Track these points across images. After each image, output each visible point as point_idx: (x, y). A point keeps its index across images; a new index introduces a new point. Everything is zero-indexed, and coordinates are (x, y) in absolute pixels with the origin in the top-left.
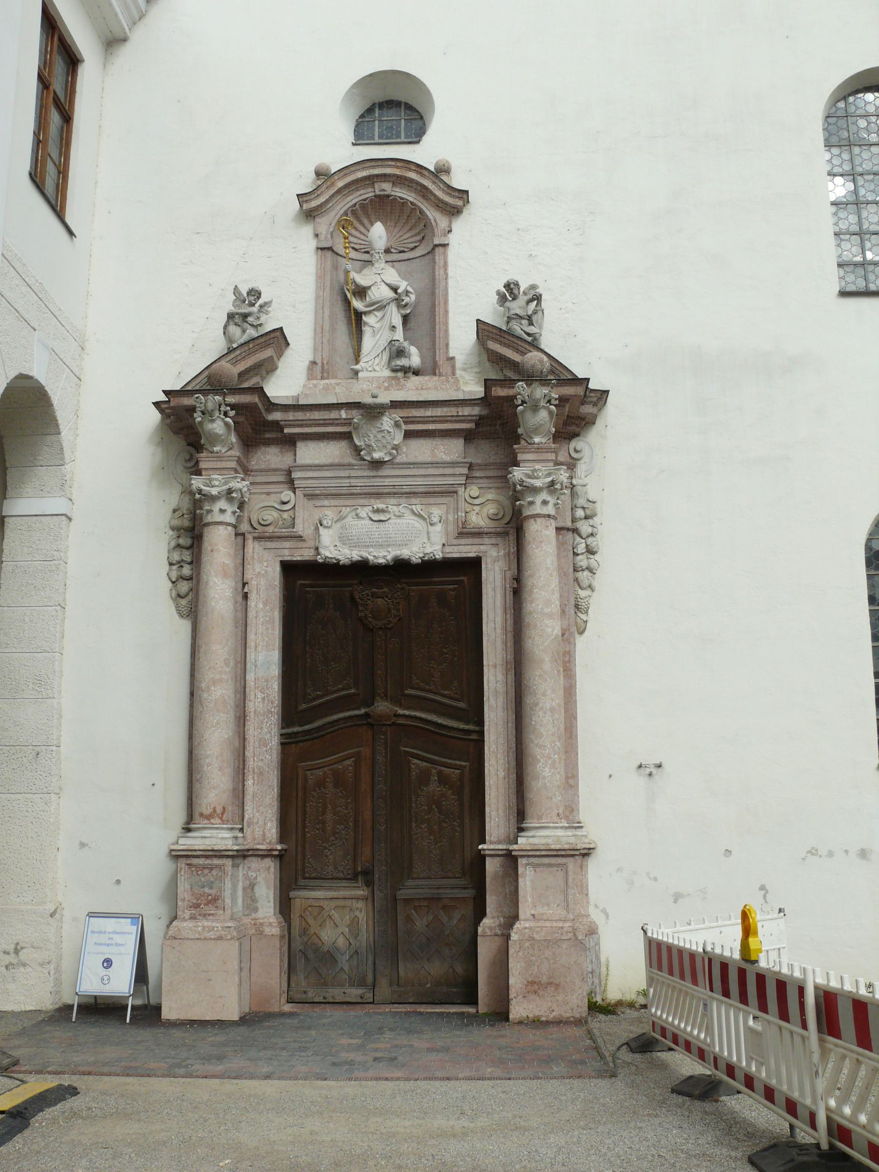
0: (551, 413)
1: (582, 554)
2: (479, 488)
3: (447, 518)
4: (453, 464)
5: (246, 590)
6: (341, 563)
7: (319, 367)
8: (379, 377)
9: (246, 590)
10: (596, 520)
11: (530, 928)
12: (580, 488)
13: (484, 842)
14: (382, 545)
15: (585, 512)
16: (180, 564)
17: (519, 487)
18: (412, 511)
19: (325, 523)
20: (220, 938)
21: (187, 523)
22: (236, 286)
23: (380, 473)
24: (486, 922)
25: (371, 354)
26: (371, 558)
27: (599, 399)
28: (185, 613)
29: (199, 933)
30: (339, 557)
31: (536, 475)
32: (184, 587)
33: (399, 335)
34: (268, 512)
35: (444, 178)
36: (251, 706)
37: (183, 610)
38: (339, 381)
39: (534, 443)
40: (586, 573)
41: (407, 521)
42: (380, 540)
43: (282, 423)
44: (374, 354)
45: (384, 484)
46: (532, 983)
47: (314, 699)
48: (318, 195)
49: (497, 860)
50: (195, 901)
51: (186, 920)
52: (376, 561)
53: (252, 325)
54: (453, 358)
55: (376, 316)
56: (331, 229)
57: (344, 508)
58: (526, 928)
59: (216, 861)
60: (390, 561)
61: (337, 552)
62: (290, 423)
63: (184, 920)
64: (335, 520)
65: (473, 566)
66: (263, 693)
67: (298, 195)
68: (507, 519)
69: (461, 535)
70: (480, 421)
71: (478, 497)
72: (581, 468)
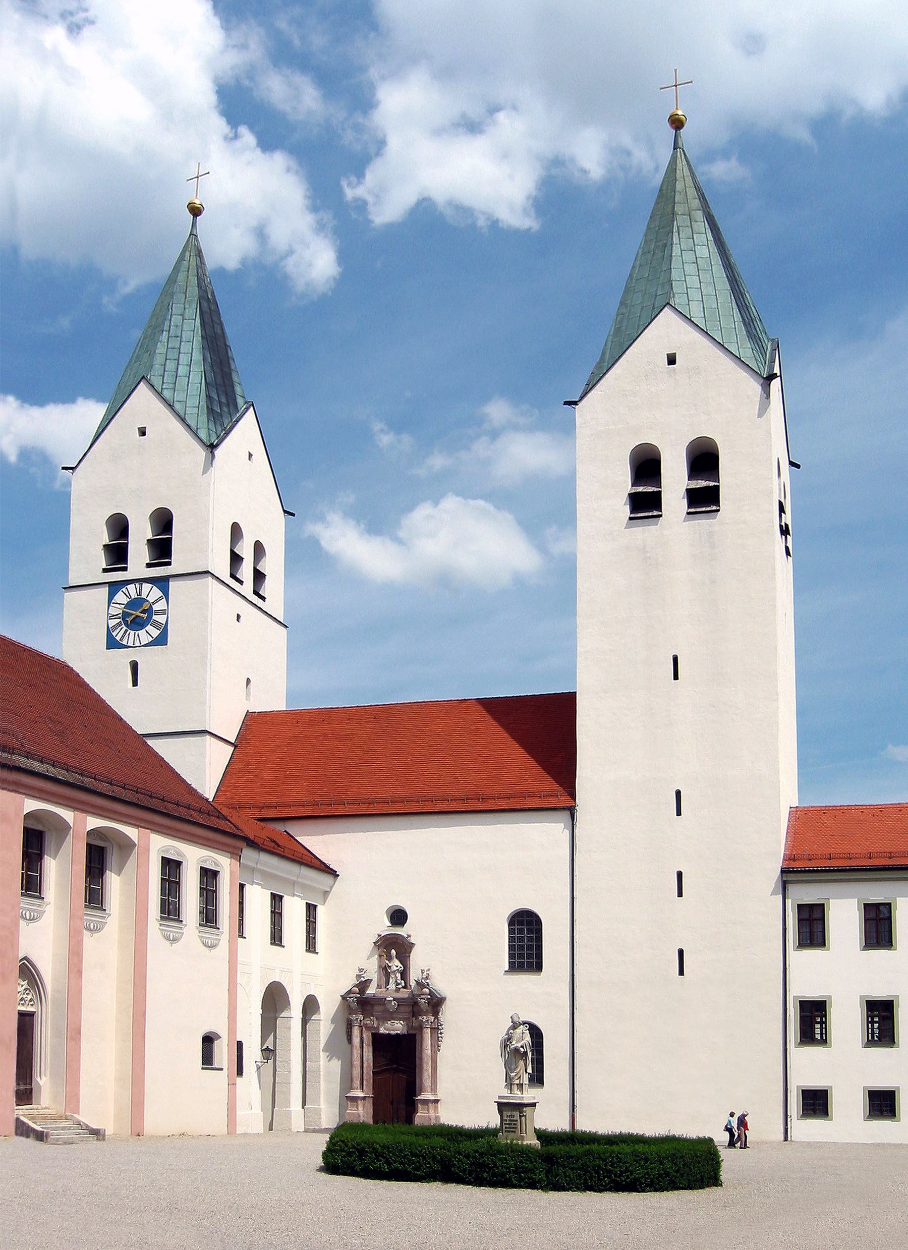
65: (415, 1035)
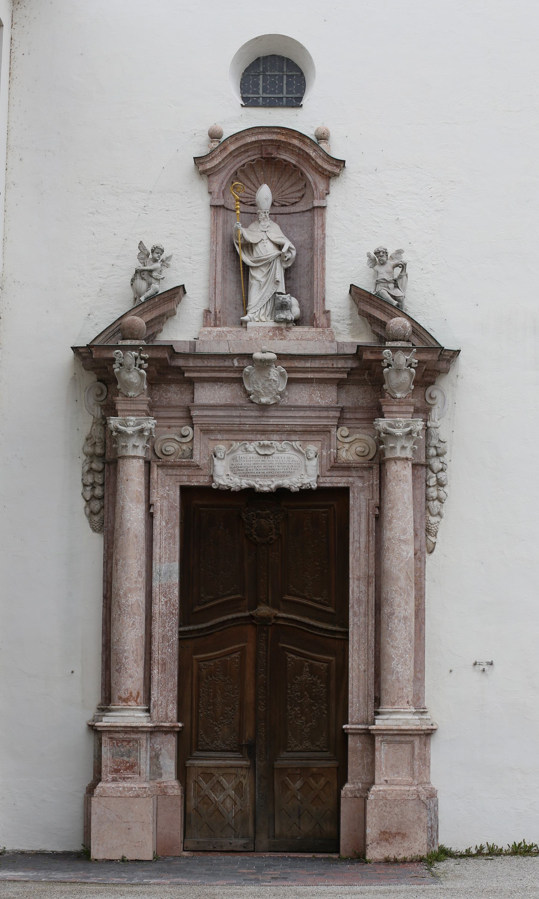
0: (411, 374)
1: (434, 486)
2: (348, 428)
3: (322, 453)
4: (327, 408)
5: (151, 511)
6: (232, 489)
7: (213, 316)
8: (265, 327)
9: (151, 511)
10: (446, 458)
11: (384, 791)
12: (433, 429)
13: (347, 723)
14: (267, 476)
15: (436, 450)
16: (93, 486)
17: (383, 435)
18: (293, 446)
19: (219, 455)
20: (138, 796)
21: (99, 450)
22: (141, 242)
23: (266, 414)
24: (348, 786)
25: (258, 306)
26: (257, 486)
27: (452, 357)
28: (97, 527)
29: (120, 792)
30: (231, 485)
31: (397, 425)
32: (96, 505)
33: (282, 288)
34: (171, 444)
35: (323, 145)
36: (156, 609)
37: (96, 525)
38: (230, 329)
39: (396, 398)
40: (436, 503)
41: (288, 455)
42: (266, 471)
43: (182, 368)
44: (260, 305)
45: (269, 423)
46: (384, 833)
47: (206, 603)
48: (213, 158)
49: (357, 738)
50: (116, 767)
51: (109, 782)
52: (261, 489)
53: (156, 279)
54: (328, 312)
55: (263, 271)
56: (223, 188)
57: (234, 442)
58: (380, 791)
59: (133, 736)
60: (273, 489)
61: (229, 480)
62: (189, 368)
63: (107, 781)
64: (227, 452)
66: (165, 597)
67: (194, 158)
68: (371, 456)
69: (333, 468)
70: (351, 372)
71: (347, 437)
72: (435, 413)
